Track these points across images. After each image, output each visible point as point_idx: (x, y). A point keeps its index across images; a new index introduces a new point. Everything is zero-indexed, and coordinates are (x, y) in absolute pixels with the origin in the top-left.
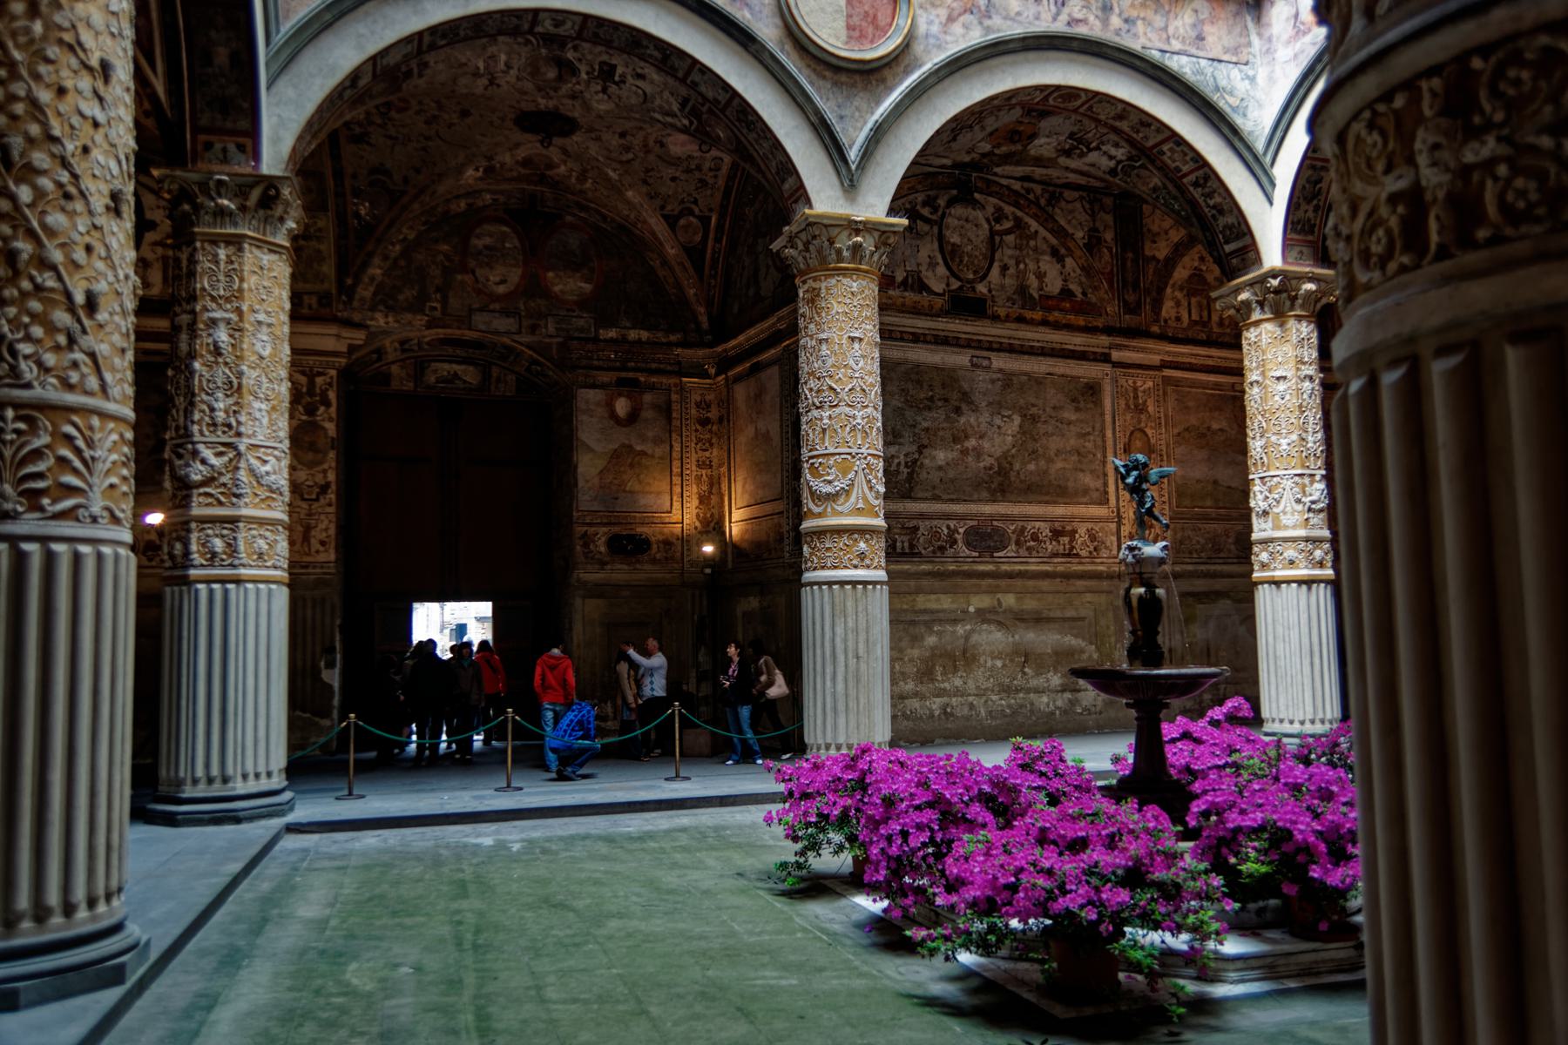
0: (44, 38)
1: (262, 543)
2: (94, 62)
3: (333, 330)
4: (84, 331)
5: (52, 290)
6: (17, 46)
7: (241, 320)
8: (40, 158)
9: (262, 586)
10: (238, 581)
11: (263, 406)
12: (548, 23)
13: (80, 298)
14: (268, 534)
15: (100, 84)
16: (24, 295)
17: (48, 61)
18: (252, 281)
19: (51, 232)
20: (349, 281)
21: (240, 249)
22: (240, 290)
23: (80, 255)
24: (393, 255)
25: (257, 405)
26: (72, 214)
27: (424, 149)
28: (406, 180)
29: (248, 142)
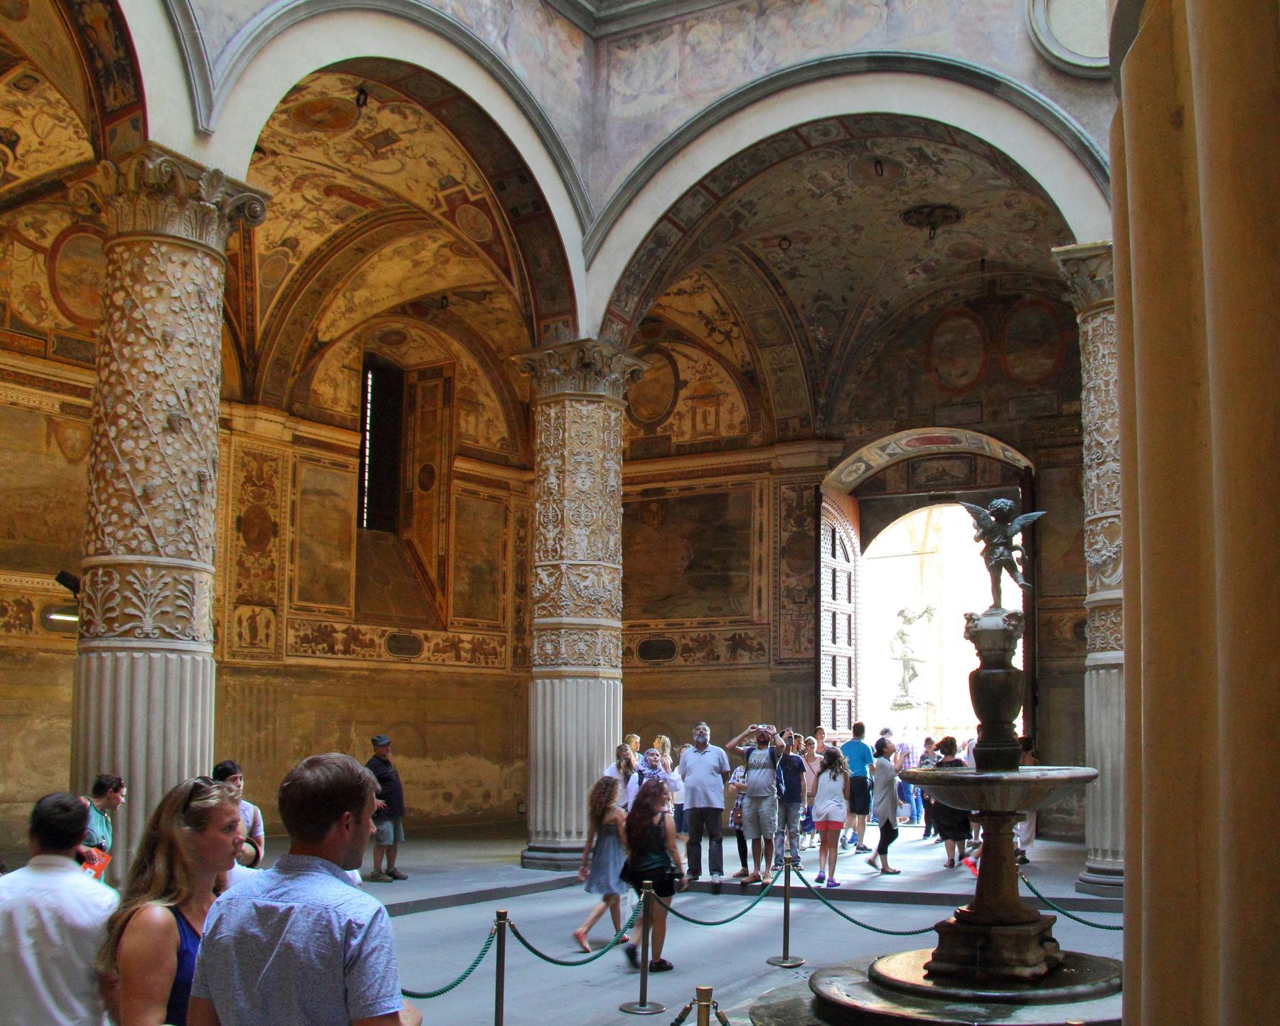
0: (128, 331)
1: (582, 646)
2: (158, 336)
3: (813, 446)
4: (141, 513)
5: (123, 490)
6: (116, 340)
7: (564, 464)
8: (122, 409)
9: (580, 681)
10: (560, 676)
11: (583, 531)
12: (814, 135)
13: (138, 492)
14: (587, 637)
15: (161, 348)
16: (110, 496)
17: (130, 344)
18: (572, 430)
19: (123, 453)
20: (822, 401)
21: (564, 407)
22: (563, 439)
23: (141, 465)
24: (865, 368)
25: (576, 531)
26: (136, 439)
27: (846, 268)
28: (844, 299)
29: (570, 317)
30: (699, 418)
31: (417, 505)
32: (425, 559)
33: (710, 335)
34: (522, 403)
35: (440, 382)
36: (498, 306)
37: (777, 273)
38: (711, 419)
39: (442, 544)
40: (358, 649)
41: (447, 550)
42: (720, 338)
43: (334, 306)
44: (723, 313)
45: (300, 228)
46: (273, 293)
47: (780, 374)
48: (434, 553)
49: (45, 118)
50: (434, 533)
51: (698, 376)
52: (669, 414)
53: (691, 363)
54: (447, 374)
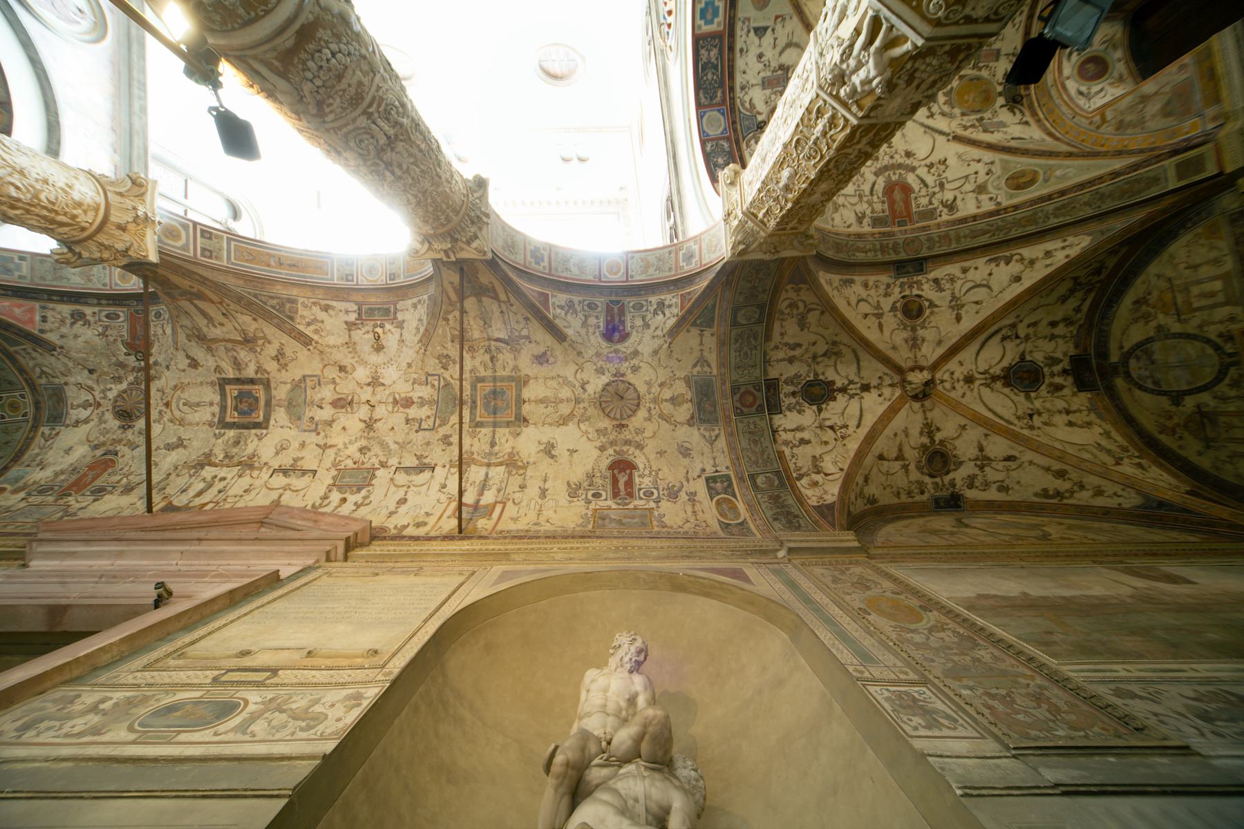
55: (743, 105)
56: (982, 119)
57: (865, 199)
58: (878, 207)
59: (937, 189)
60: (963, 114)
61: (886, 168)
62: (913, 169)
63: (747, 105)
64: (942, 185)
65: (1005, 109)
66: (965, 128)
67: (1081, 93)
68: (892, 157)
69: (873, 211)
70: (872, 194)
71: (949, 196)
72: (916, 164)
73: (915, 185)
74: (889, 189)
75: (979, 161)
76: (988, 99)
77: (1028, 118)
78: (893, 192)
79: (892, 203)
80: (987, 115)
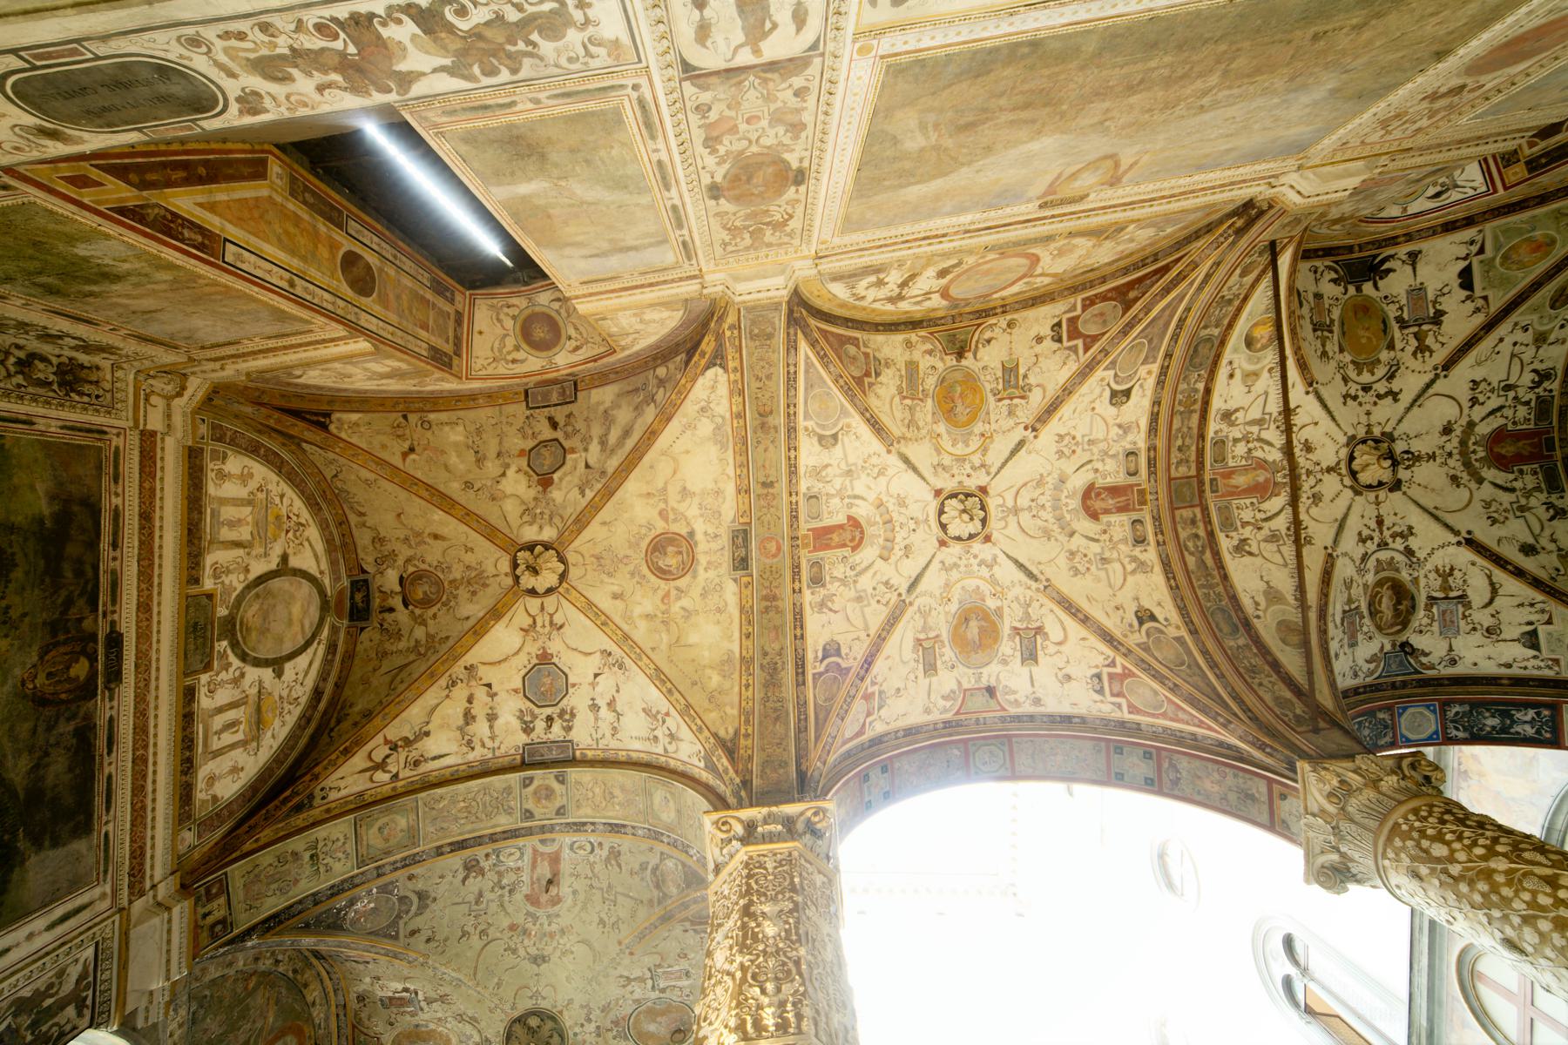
27: (465, 934)
30: (231, 715)
31: (323, 227)
32: (222, 193)
33: (386, 742)
34: (328, 415)
35: (448, 348)
36: (511, 472)
37: (480, 852)
38: (228, 738)
39: (250, 263)
40: (314, 43)
41: (234, 271)
42: (378, 756)
43: (725, 402)
44: (416, 763)
45: (834, 463)
46: (809, 386)
47: (307, 856)
48: (232, 231)
49: (1101, 436)
50: (270, 250)
51: (285, 694)
52: (244, 657)
53: (300, 677)
54: (456, 361)
55: (1372, 673)
56: (1399, 320)
57: (1523, 501)
58: (1530, 481)
59: (1511, 394)
60: (1391, 347)
61: (1467, 465)
62: (1471, 425)
63: (1372, 666)
64: (1508, 388)
65: (1381, 283)
66: (1422, 349)
67: (1438, 195)
68: (1450, 455)
69: (1538, 489)
70: (1513, 490)
71: (1528, 378)
72: (1464, 421)
73: (1495, 422)
74: (1502, 463)
75: (1501, 340)
76: (1363, 309)
77: (1403, 250)
78: (1504, 457)
79: (1520, 459)
80: (1392, 311)
